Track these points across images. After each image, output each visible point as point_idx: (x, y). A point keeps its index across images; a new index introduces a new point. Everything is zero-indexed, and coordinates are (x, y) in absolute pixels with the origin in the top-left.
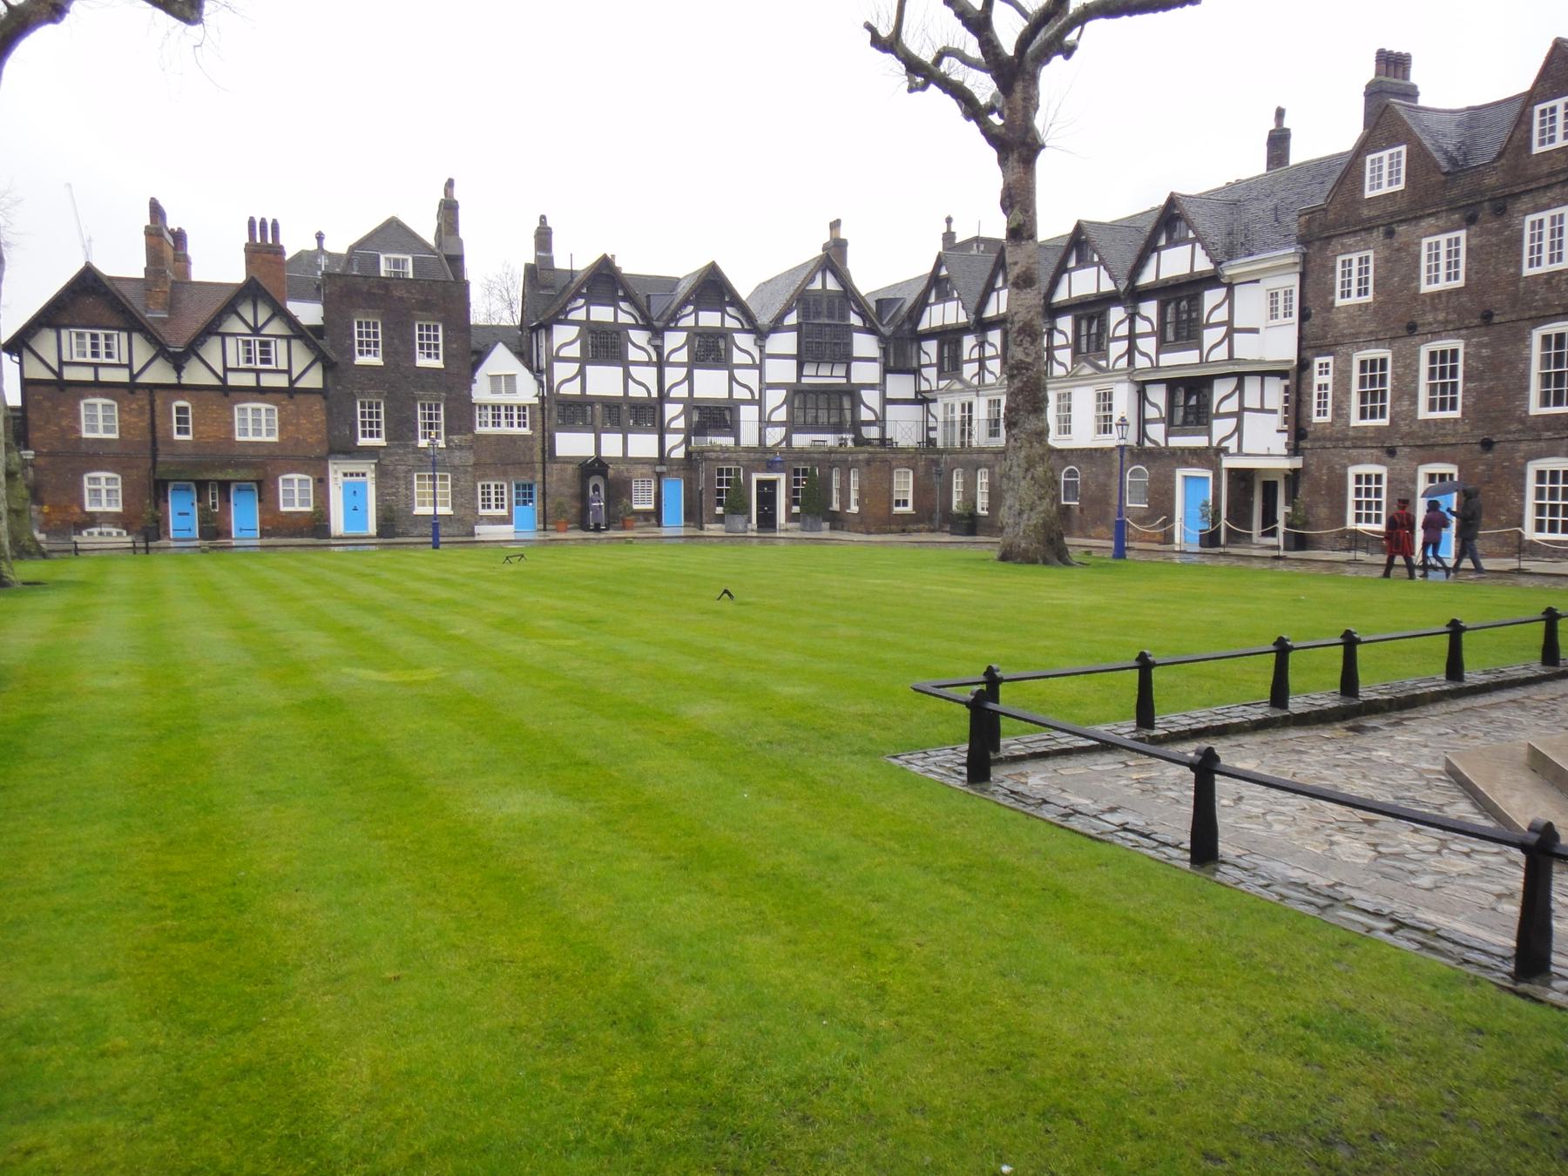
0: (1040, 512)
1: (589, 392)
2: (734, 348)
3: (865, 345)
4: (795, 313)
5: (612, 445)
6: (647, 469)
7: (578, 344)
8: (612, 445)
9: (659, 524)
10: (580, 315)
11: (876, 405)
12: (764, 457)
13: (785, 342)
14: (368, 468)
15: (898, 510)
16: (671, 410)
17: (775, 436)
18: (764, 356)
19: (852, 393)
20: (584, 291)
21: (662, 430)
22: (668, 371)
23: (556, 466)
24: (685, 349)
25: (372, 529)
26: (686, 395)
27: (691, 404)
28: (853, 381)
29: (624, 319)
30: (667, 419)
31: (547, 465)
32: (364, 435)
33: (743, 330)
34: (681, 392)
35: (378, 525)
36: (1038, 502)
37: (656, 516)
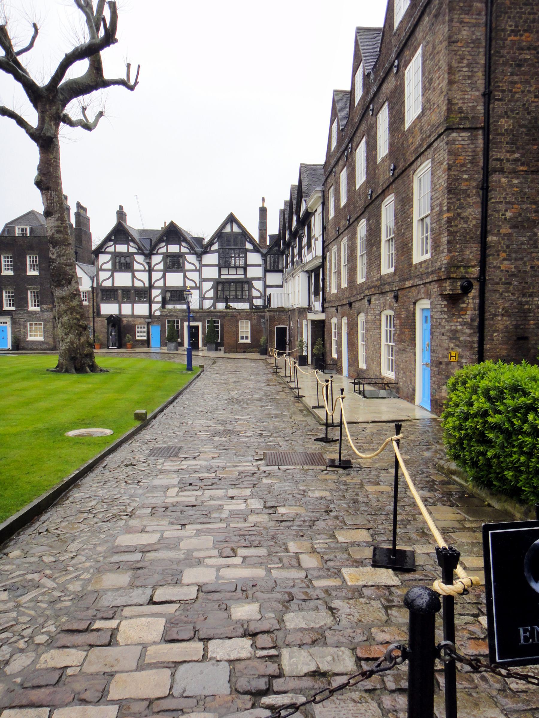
0: (67, 343)
1: (115, 285)
2: (186, 263)
3: (254, 258)
4: (217, 244)
5: (127, 309)
6: (142, 321)
7: (110, 262)
8: (127, 309)
9: (149, 346)
10: (111, 249)
11: (261, 288)
12: (201, 314)
13: (212, 258)
14: (8, 319)
15: (241, 341)
16: (156, 293)
17: (207, 304)
18: (202, 265)
19: (248, 282)
20: (113, 238)
21: (151, 302)
22: (154, 274)
23: (99, 319)
24: (162, 263)
25: (10, 346)
26: (162, 285)
27: (165, 290)
28: (248, 276)
29: (132, 250)
30: (153, 297)
31: (96, 319)
32: (32, 306)
33: (190, 253)
34: (160, 284)
35: (12, 346)
36: (65, 337)
37: (147, 343)
